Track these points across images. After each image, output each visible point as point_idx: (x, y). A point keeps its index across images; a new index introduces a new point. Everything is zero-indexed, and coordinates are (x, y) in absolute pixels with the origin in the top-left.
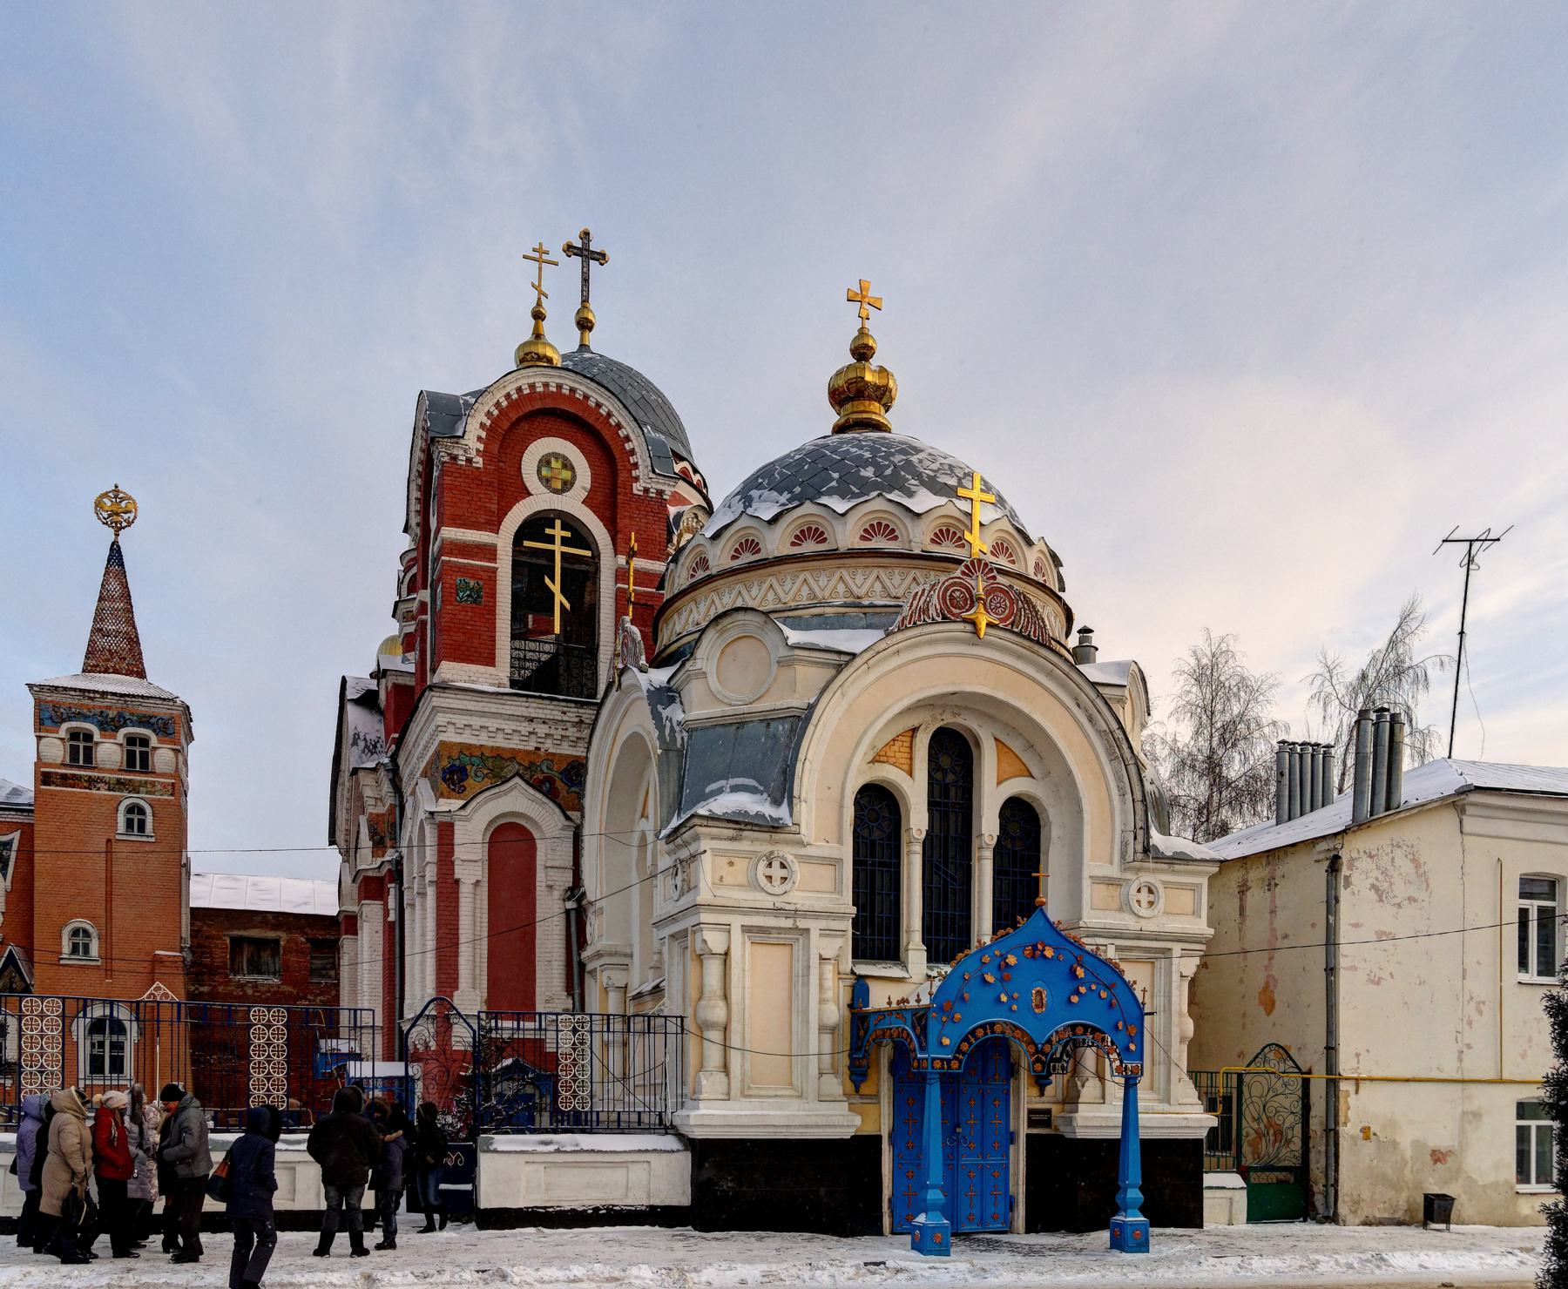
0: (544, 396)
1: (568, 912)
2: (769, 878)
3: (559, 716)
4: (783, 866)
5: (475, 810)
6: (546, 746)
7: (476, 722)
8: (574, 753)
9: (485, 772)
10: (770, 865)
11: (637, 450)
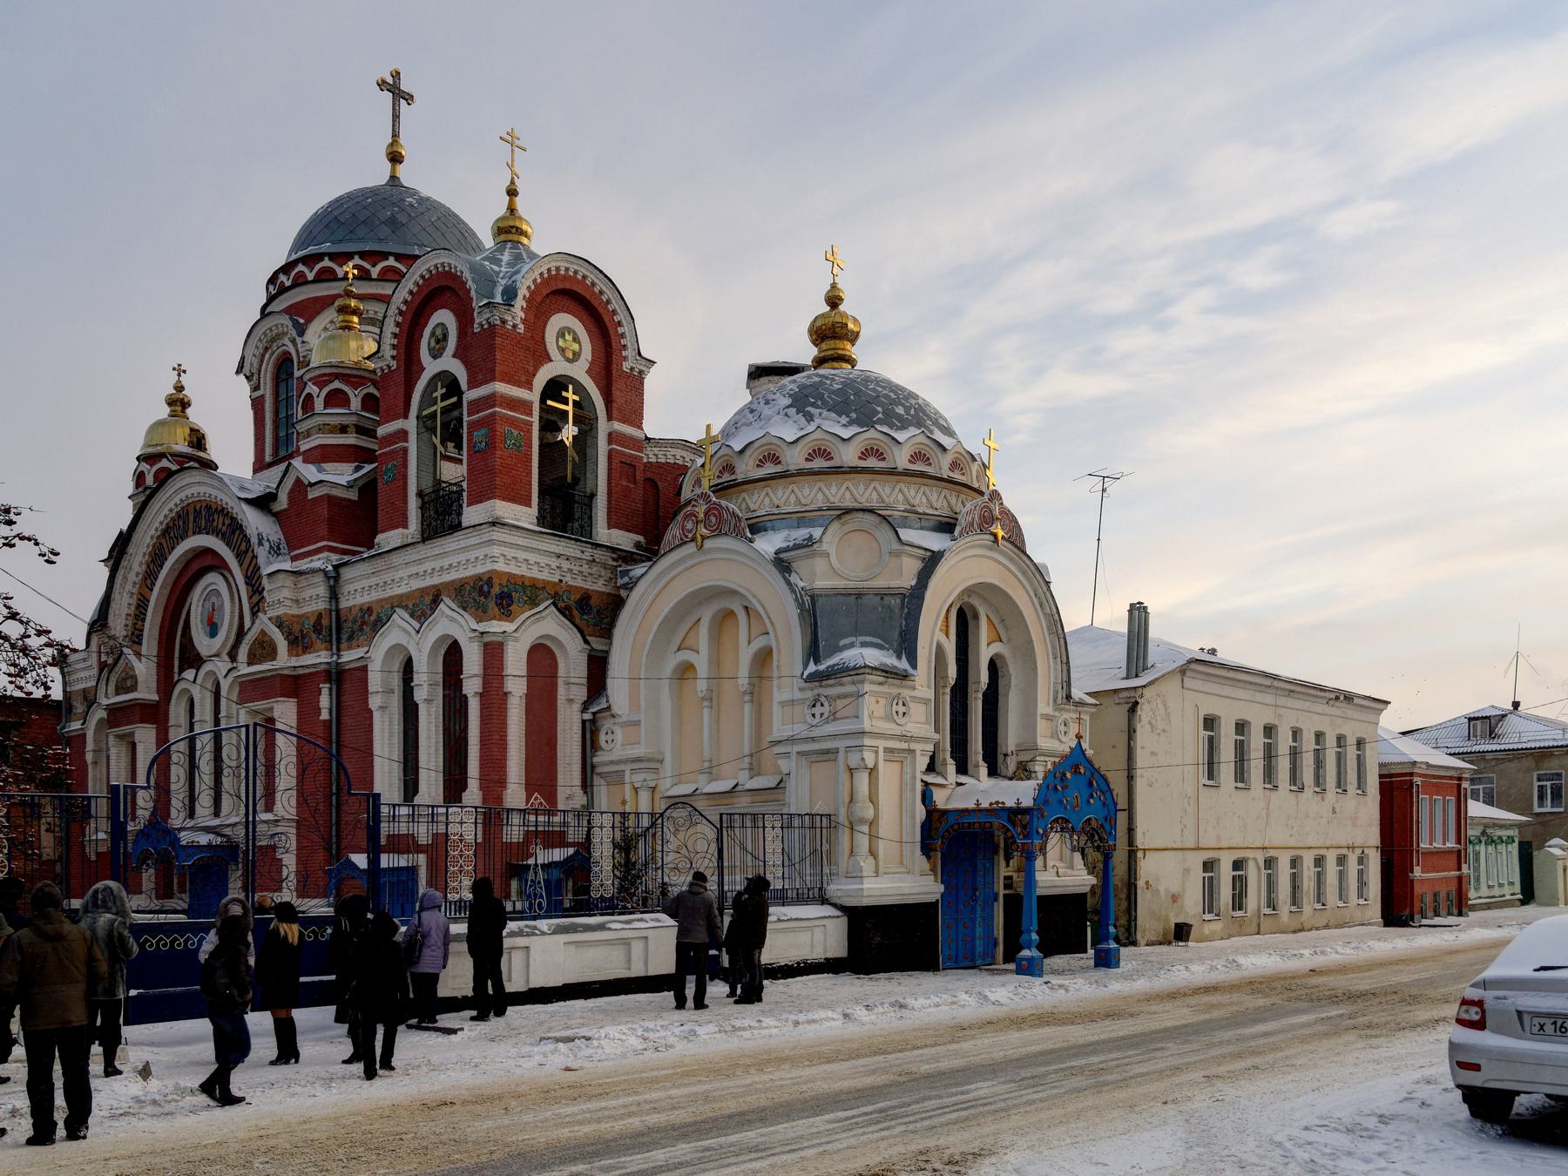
0: (566, 278)
1: (584, 722)
3: (579, 555)
7: (521, 555)
11: (627, 334)
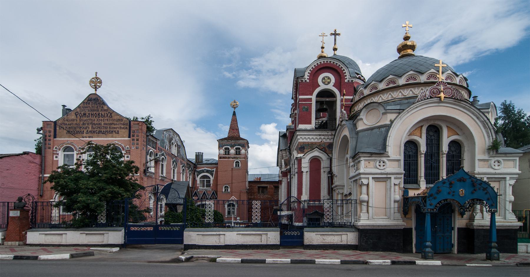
2: (380, 166)
3: (326, 134)
4: (383, 162)
5: (306, 156)
6: (324, 140)
8: (330, 141)
9: (309, 147)
10: (380, 162)
